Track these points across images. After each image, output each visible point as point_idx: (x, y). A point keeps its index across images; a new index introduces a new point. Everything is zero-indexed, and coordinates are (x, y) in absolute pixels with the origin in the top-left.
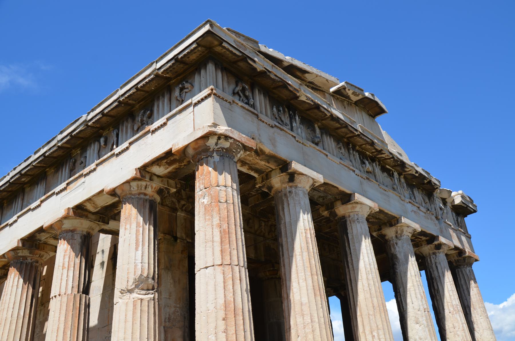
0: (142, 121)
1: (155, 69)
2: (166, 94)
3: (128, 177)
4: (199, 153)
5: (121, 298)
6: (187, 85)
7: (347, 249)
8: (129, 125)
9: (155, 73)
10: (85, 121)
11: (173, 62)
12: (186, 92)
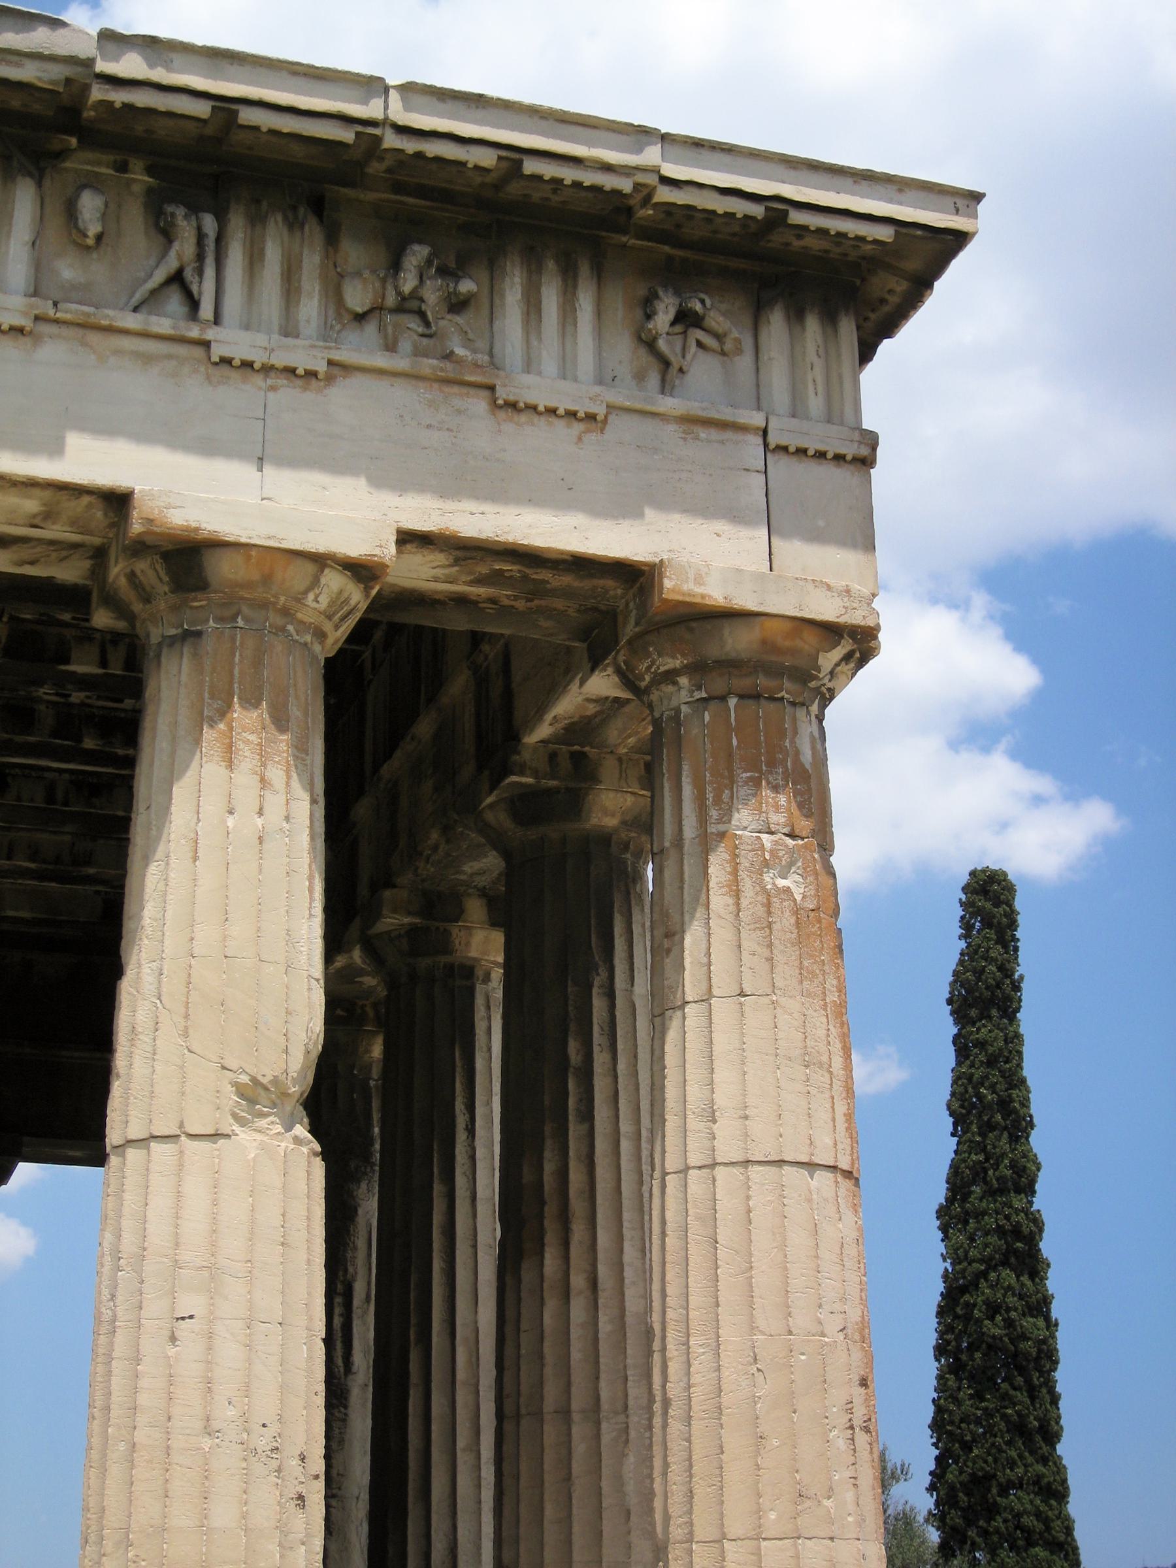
0: (415, 295)
1: (656, 170)
2: (585, 270)
3: (355, 548)
4: (776, 671)
5: (242, 1122)
6: (716, 320)
7: (459, 1106)
8: (312, 260)
9: (641, 178)
10: (89, 63)
11: (757, 211)
12: (699, 344)
